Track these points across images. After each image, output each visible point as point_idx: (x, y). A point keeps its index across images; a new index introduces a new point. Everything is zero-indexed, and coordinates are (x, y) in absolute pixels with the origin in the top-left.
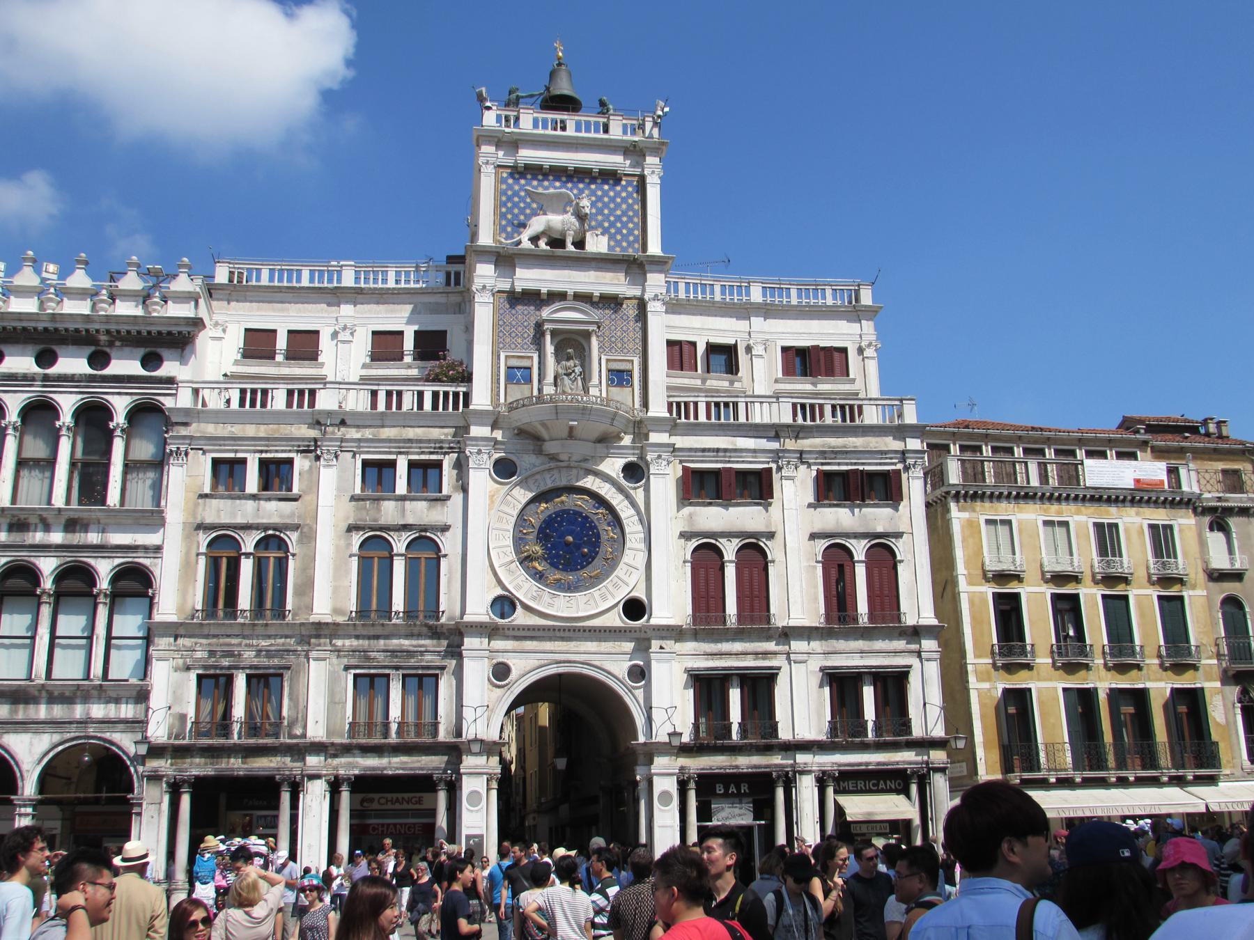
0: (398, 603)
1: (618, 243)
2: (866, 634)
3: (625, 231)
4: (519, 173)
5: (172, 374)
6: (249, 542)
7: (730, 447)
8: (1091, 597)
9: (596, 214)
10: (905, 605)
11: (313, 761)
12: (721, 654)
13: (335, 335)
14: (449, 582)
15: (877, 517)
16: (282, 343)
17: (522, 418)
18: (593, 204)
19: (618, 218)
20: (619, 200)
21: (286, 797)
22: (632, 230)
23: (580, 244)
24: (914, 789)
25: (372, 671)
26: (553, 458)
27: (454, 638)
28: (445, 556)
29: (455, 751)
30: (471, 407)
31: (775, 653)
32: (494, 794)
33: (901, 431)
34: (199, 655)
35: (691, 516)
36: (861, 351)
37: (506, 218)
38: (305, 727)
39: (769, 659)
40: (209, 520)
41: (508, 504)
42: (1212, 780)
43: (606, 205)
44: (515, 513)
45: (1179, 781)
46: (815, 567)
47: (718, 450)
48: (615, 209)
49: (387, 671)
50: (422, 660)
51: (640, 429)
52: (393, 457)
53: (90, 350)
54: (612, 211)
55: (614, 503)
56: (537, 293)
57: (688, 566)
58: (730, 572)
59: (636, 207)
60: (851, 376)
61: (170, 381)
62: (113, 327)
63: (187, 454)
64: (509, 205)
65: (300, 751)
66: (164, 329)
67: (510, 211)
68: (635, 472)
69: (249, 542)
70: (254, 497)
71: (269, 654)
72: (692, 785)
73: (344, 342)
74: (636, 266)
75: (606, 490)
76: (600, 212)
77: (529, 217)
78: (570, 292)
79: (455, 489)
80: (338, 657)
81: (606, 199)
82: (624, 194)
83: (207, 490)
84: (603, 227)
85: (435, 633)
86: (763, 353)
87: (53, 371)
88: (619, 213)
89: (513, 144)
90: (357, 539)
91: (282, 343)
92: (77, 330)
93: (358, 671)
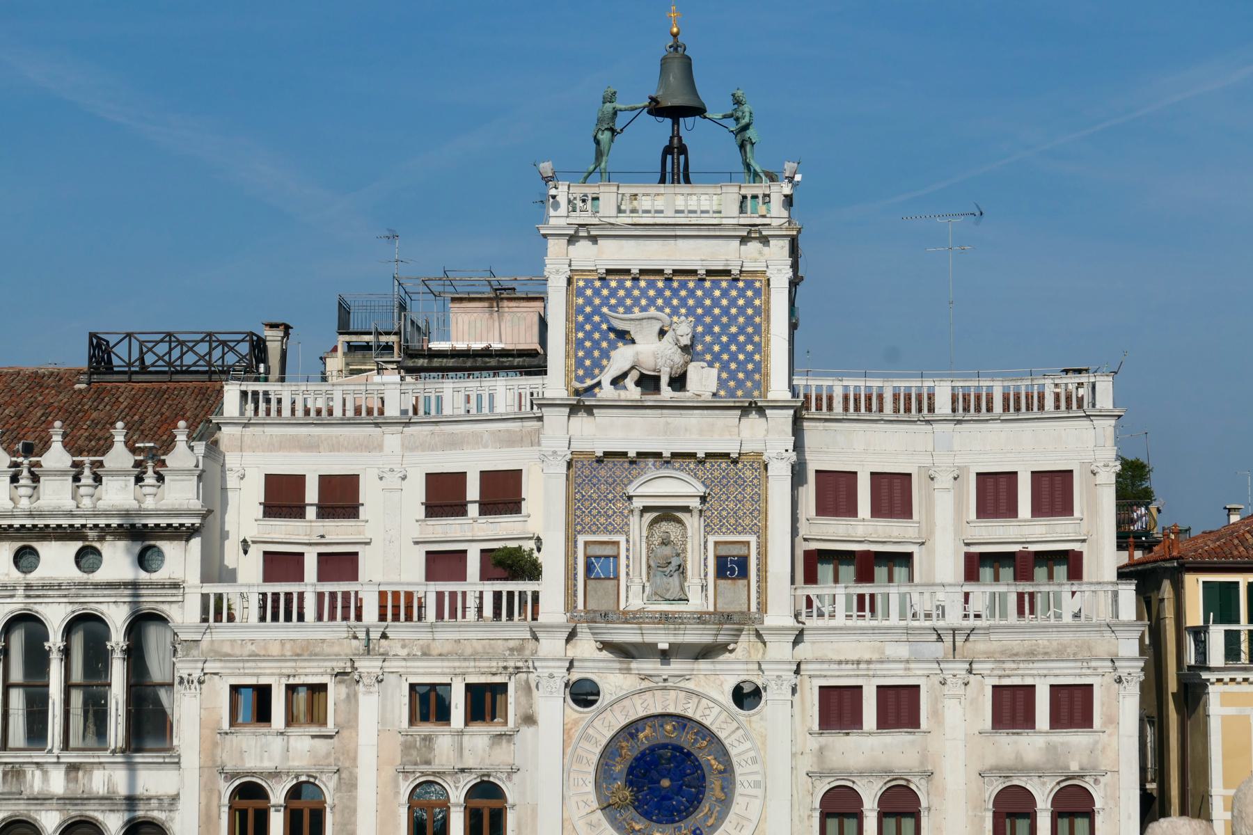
1: (733, 375)
3: (741, 357)
4: (600, 279)
5: (178, 576)
6: (277, 794)
7: (875, 657)
9: (703, 335)
16: (312, 494)
18: (699, 320)
19: (733, 338)
20: (734, 311)
22: (752, 354)
23: (679, 382)
28: (513, 806)
30: (542, 618)
35: (821, 750)
37: (583, 348)
41: (589, 738)
43: (716, 320)
44: (598, 750)
46: (983, 819)
47: (858, 662)
48: (727, 326)
52: (446, 680)
53: (76, 545)
54: (725, 328)
55: (722, 735)
56: (625, 454)
59: (757, 320)
60: (1077, 513)
61: (175, 586)
62: (102, 522)
63: (201, 682)
64: (588, 327)
66: (163, 522)
67: (588, 335)
69: (277, 794)
70: (282, 734)
73: (391, 490)
76: (708, 330)
77: (613, 346)
78: (667, 454)
81: (717, 311)
82: (741, 302)
83: (225, 725)
84: (712, 353)
87: (34, 577)
88: (734, 329)
90: (405, 788)
91: (312, 494)
92: (59, 526)
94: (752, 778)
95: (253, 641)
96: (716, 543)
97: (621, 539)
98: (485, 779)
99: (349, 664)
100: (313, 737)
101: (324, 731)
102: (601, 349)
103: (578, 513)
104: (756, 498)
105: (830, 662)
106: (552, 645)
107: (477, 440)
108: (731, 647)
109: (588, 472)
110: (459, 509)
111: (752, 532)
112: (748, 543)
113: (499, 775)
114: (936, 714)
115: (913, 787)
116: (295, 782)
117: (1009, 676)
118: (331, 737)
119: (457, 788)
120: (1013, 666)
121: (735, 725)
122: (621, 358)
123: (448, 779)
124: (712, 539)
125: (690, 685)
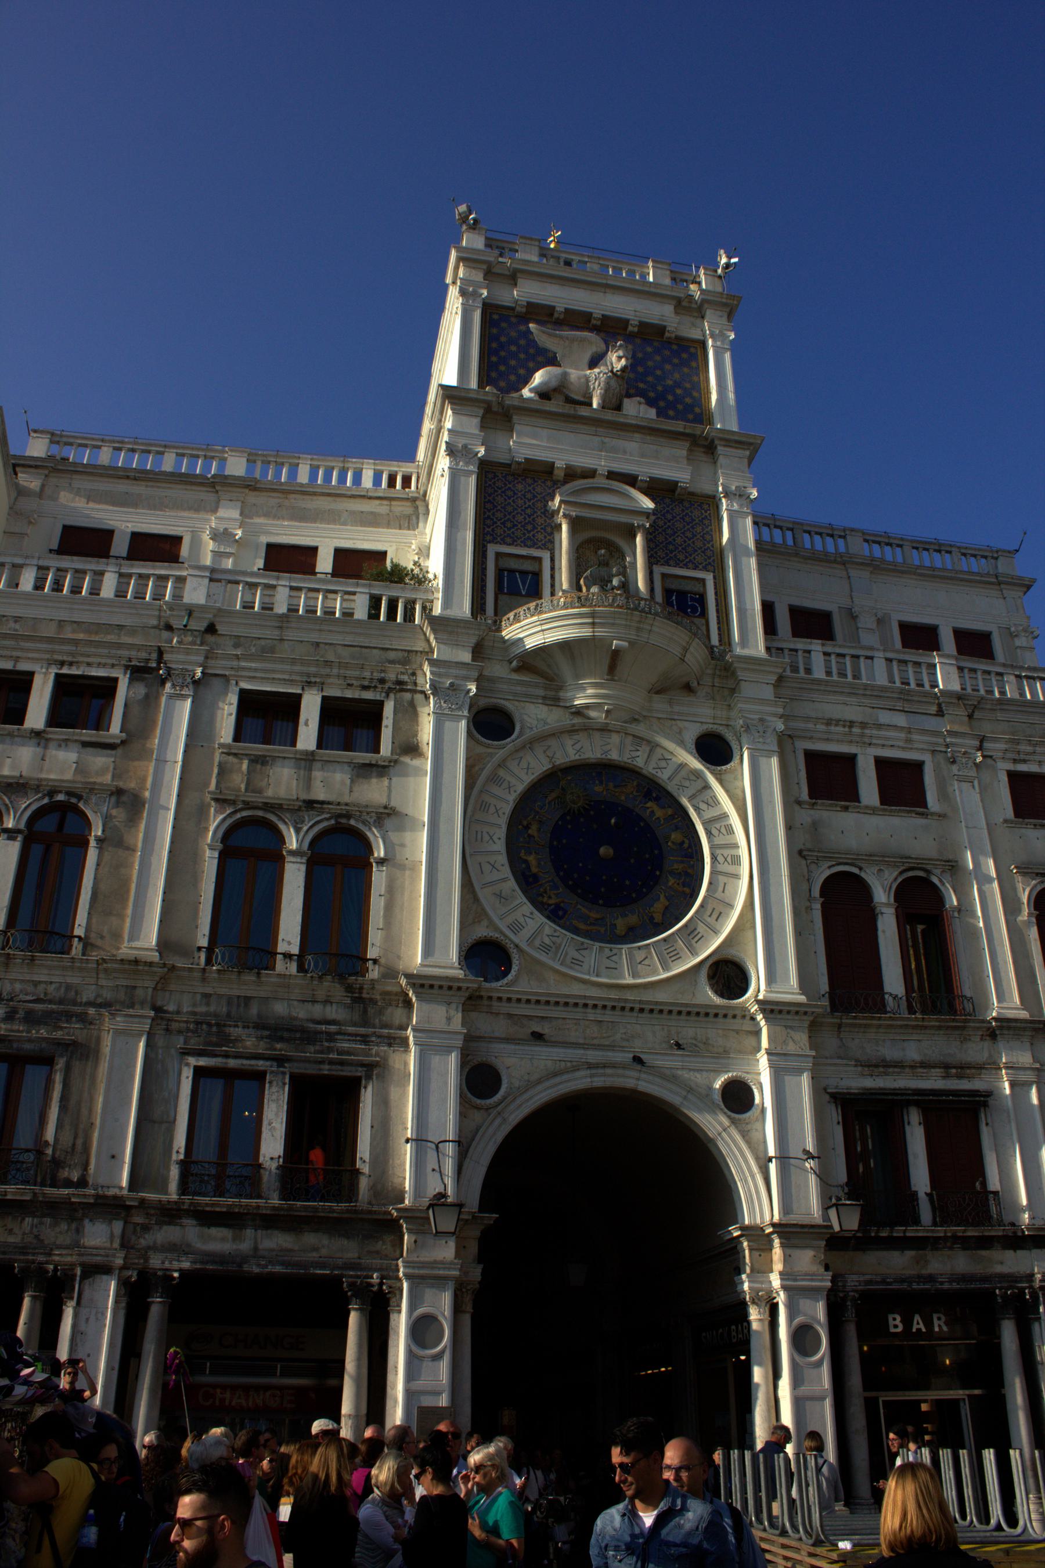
3: (680, 407)
11: (99, 1235)
12: (884, 1066)
14: (389, 908)
25: (232, 1063)
28: (381, 862)
31: (980, 1068)
32: (467, 1319)
35: (815, 825)
38: (86, 1166)
39: (969, 1077)
44: (512, 798)
47: (852, 724)
49: (261, 1065)
50: (330, 1050)
57: (817, 906)
70: (37, 734)
71: (31, 1019)
72: (850, 1314)
80: (167, 1030)
86: (874, 626)
93: (202, 1062)
94: (727, 852)
95: (17, 619)
96: (664, 576)
97: (546, 556)
98: (343, 821)
99: (154, 656)
100: (86, 744)
101: (101, 736)
102: (519, 376)
103: (488, 522)
104: (708, 537)
105: (817, 720)
107: (333, 518)
108: (694, 684)
109: (499, 484)
111: (705, 569)
112: (703, 581)
113: (365, 817)
114: (944, 795)
115: (935, 880)
116: (46, 801)
117: (1025, 761)
118: (111, 747)
119: (298, 831)
120: (1029, 749)
121: (699, 784)
123: (287, 816)
124: (658, 570)
125: (640, 729)
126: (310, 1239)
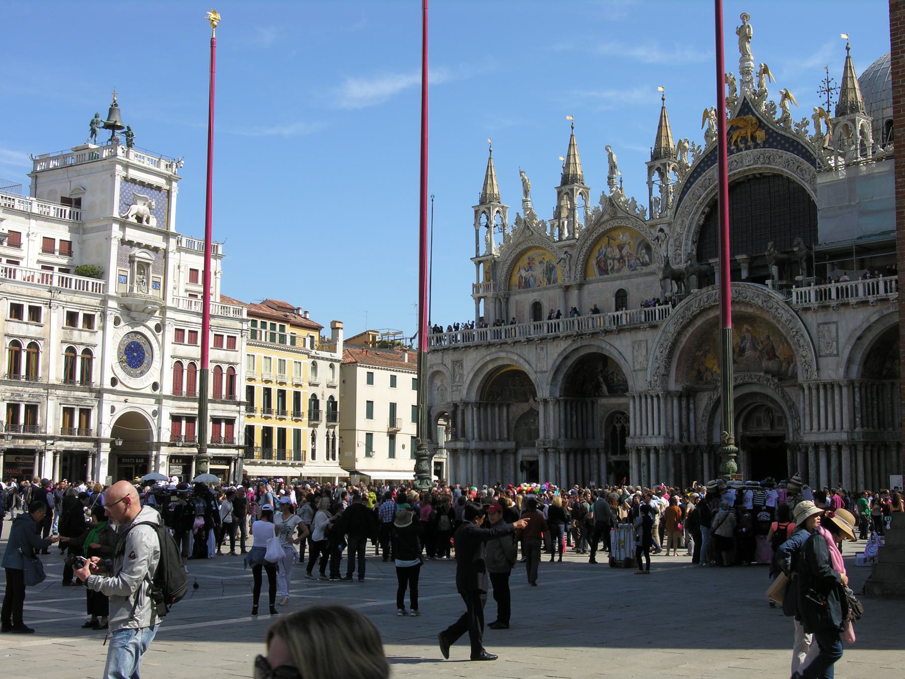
0: (78, 377)
2: (224, 402)
6: (25, 344)
8: (275, 388)
10: (237, 393)
13: (28, 235)
15: (231, 356)
17: (128, 301)
21: (37, 458)
24: (233, 464)
26: (133, 319)
27: (99, 393)
29: (97, 442)
33: (242, 321)
34: (8, 394)
36: (215, 274)
40: (11, 333)
42: (301, 465)
45: (293, 465)
51: (164, 310)
58: (185, 373)
65: (44, 439)
68: (158, 328)
69: (25, 346)
74: (167, 235)
75: (149, 334)
79: (99, 328)
85: (91, 391)
89: (127, 166)
106: (112, 304)
110: (52, 252)
122: (134, 209)
126: (83, 443)
